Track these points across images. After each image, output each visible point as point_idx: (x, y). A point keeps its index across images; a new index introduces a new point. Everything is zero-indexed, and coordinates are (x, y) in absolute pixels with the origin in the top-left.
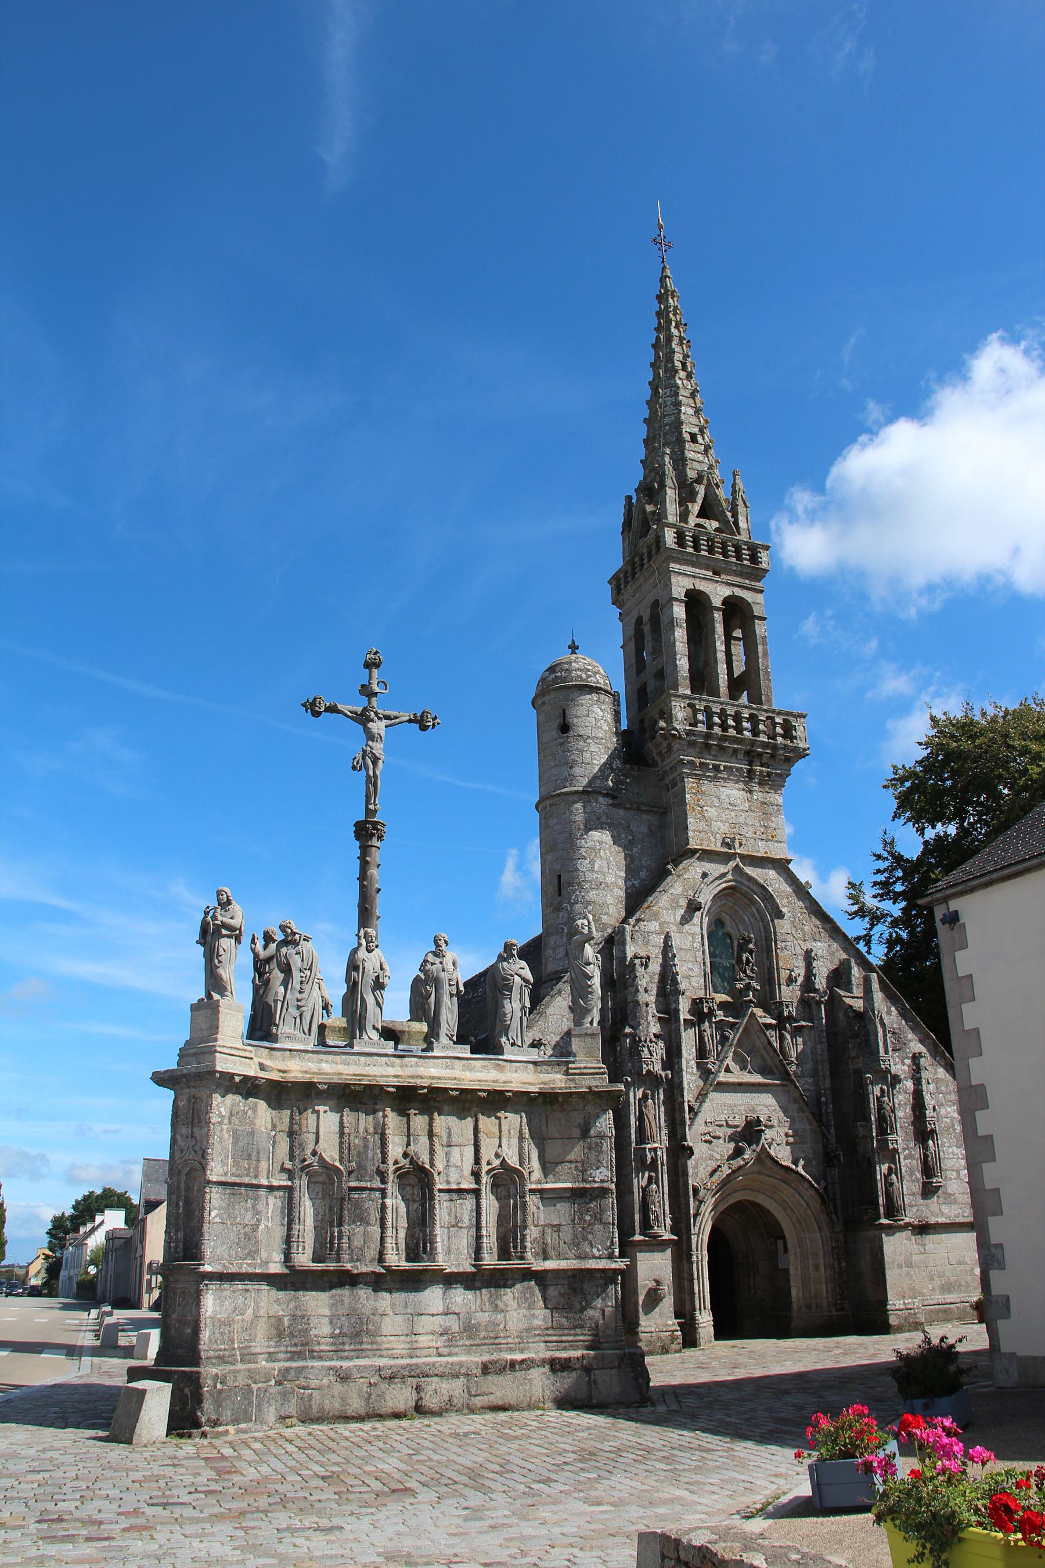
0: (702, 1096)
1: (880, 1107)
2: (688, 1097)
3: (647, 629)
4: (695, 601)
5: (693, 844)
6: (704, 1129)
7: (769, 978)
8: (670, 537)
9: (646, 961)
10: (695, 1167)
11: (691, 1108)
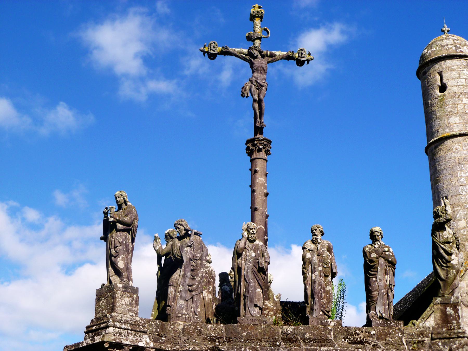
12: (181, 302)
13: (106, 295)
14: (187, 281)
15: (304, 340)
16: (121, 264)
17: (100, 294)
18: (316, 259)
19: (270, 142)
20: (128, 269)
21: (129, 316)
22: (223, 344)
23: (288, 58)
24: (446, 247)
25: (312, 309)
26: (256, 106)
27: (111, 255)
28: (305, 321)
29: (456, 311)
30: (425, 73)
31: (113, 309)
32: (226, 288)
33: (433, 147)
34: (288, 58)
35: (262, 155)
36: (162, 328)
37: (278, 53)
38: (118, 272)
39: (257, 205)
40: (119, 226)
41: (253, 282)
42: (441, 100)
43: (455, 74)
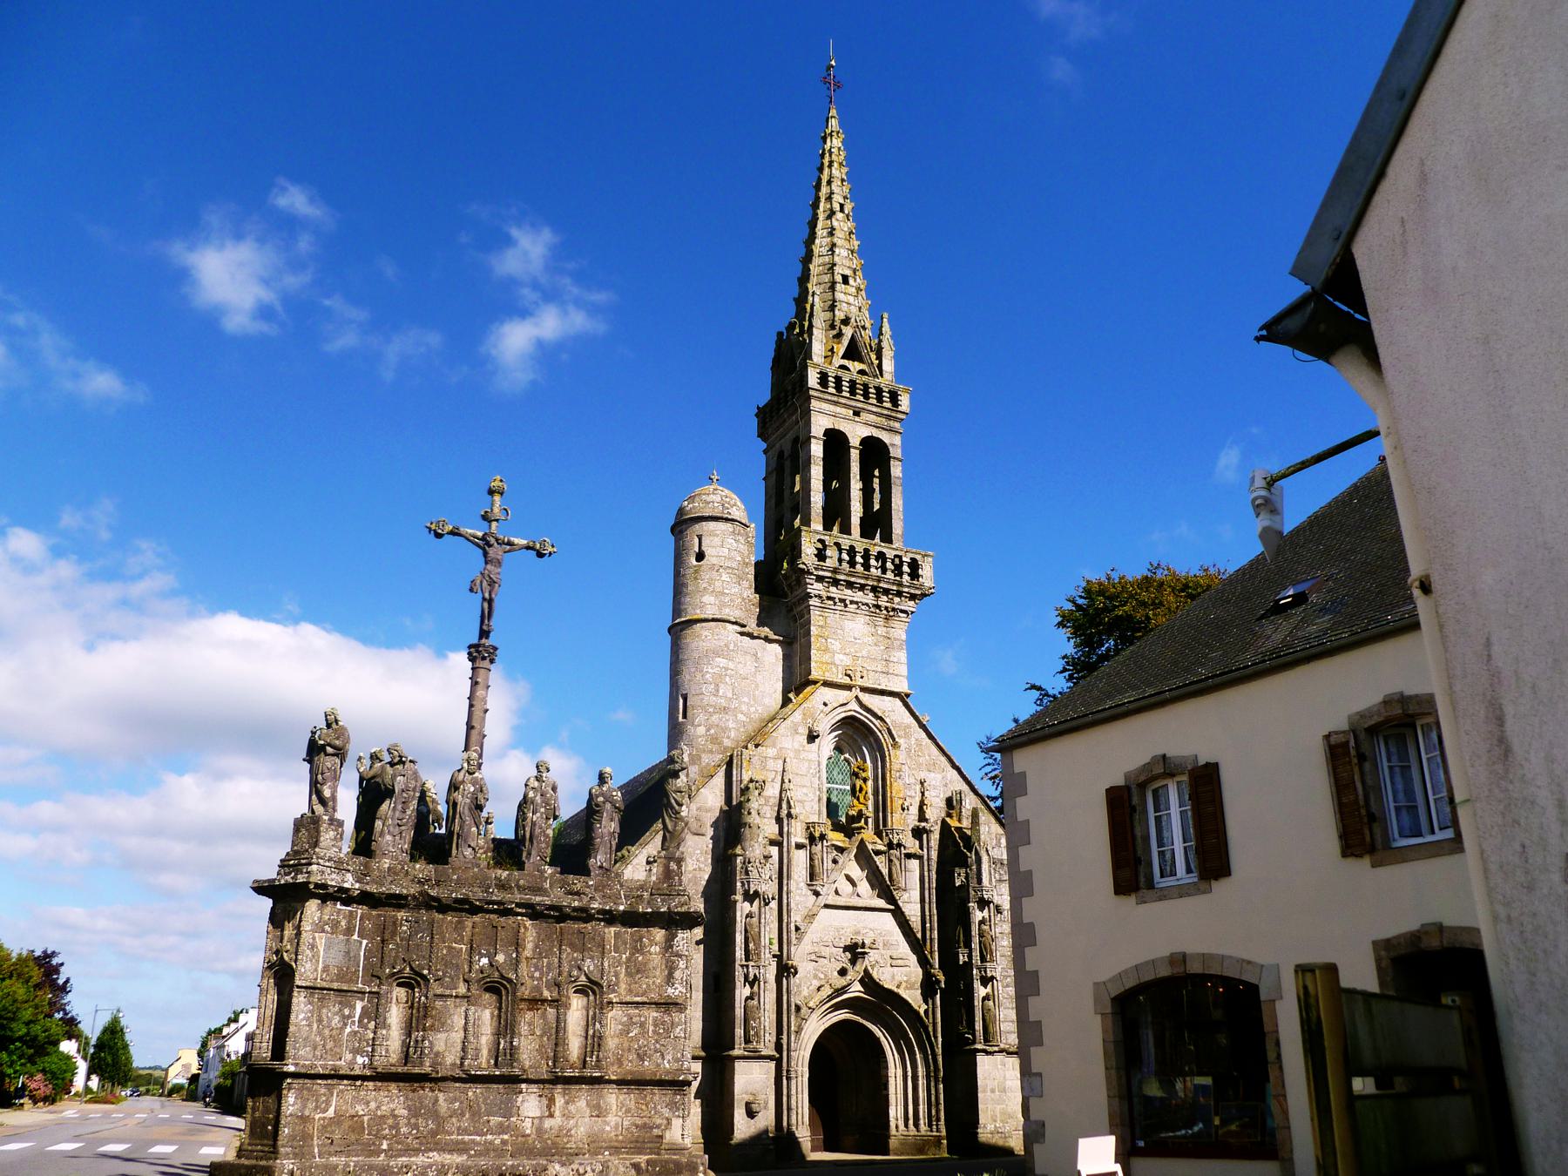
0: (811, 917)
1: (981, 935)
2: (796, 918)
3: (788, 464)
4: (835, 441)
5: (815, 675)
6: (809, 948)
7: (882, 807)
8: (813, 379)
9: (761, 785)
10: (799, 986)
11: (797, 929)
12: (388, 838)
13: (307, 827)
14: (397, 814)
15: (518, 886)
16: (327, 793)
17: (299, 824)
18: (538, 799)
19: (495, 649)
20: (334, 798)
21: (332, 853)
22: (432, 887)
23: (528, 548)
24: (678, 796)
25: (529, 854)
26: (486, 605)
27: (317, 782)
28: (520, 866)
29: (680, 867)
30: (681, 532)
31: (316, 844)
32: (423, 808)
33: (679, 629)
34: (528, 548)
35: (486, 664)
36: (366, 866)
37: (516, 541)
38: (322, 801)
39: (474, 724)
40: (329, 749)
41: (468, 819)
42: (696, 572)
43: (717, 541)
